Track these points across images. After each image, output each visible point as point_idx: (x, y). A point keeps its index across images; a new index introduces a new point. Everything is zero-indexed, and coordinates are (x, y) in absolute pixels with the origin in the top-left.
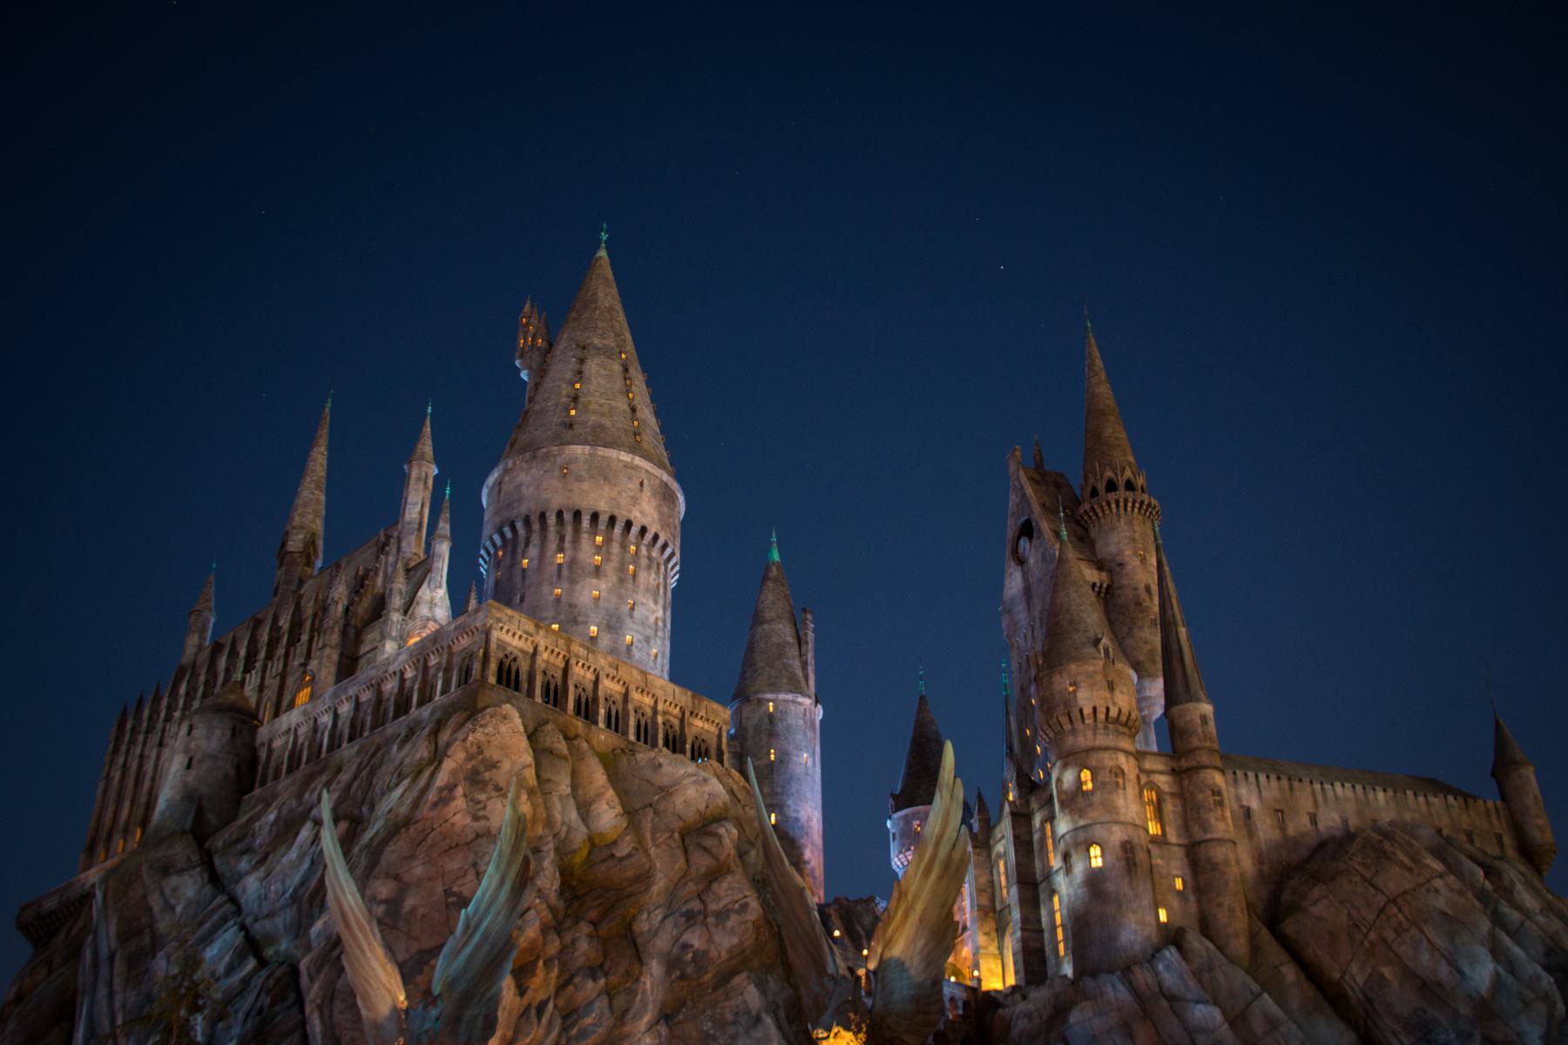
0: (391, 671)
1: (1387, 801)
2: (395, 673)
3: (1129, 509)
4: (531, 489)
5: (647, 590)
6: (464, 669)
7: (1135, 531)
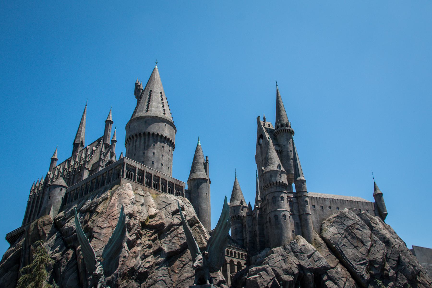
0: (100, 174)
1: (348, 203)
2: (101, 175)
3: (287, 132)
4: (137, 127)
5: (166, 152)
6: (118, 174)
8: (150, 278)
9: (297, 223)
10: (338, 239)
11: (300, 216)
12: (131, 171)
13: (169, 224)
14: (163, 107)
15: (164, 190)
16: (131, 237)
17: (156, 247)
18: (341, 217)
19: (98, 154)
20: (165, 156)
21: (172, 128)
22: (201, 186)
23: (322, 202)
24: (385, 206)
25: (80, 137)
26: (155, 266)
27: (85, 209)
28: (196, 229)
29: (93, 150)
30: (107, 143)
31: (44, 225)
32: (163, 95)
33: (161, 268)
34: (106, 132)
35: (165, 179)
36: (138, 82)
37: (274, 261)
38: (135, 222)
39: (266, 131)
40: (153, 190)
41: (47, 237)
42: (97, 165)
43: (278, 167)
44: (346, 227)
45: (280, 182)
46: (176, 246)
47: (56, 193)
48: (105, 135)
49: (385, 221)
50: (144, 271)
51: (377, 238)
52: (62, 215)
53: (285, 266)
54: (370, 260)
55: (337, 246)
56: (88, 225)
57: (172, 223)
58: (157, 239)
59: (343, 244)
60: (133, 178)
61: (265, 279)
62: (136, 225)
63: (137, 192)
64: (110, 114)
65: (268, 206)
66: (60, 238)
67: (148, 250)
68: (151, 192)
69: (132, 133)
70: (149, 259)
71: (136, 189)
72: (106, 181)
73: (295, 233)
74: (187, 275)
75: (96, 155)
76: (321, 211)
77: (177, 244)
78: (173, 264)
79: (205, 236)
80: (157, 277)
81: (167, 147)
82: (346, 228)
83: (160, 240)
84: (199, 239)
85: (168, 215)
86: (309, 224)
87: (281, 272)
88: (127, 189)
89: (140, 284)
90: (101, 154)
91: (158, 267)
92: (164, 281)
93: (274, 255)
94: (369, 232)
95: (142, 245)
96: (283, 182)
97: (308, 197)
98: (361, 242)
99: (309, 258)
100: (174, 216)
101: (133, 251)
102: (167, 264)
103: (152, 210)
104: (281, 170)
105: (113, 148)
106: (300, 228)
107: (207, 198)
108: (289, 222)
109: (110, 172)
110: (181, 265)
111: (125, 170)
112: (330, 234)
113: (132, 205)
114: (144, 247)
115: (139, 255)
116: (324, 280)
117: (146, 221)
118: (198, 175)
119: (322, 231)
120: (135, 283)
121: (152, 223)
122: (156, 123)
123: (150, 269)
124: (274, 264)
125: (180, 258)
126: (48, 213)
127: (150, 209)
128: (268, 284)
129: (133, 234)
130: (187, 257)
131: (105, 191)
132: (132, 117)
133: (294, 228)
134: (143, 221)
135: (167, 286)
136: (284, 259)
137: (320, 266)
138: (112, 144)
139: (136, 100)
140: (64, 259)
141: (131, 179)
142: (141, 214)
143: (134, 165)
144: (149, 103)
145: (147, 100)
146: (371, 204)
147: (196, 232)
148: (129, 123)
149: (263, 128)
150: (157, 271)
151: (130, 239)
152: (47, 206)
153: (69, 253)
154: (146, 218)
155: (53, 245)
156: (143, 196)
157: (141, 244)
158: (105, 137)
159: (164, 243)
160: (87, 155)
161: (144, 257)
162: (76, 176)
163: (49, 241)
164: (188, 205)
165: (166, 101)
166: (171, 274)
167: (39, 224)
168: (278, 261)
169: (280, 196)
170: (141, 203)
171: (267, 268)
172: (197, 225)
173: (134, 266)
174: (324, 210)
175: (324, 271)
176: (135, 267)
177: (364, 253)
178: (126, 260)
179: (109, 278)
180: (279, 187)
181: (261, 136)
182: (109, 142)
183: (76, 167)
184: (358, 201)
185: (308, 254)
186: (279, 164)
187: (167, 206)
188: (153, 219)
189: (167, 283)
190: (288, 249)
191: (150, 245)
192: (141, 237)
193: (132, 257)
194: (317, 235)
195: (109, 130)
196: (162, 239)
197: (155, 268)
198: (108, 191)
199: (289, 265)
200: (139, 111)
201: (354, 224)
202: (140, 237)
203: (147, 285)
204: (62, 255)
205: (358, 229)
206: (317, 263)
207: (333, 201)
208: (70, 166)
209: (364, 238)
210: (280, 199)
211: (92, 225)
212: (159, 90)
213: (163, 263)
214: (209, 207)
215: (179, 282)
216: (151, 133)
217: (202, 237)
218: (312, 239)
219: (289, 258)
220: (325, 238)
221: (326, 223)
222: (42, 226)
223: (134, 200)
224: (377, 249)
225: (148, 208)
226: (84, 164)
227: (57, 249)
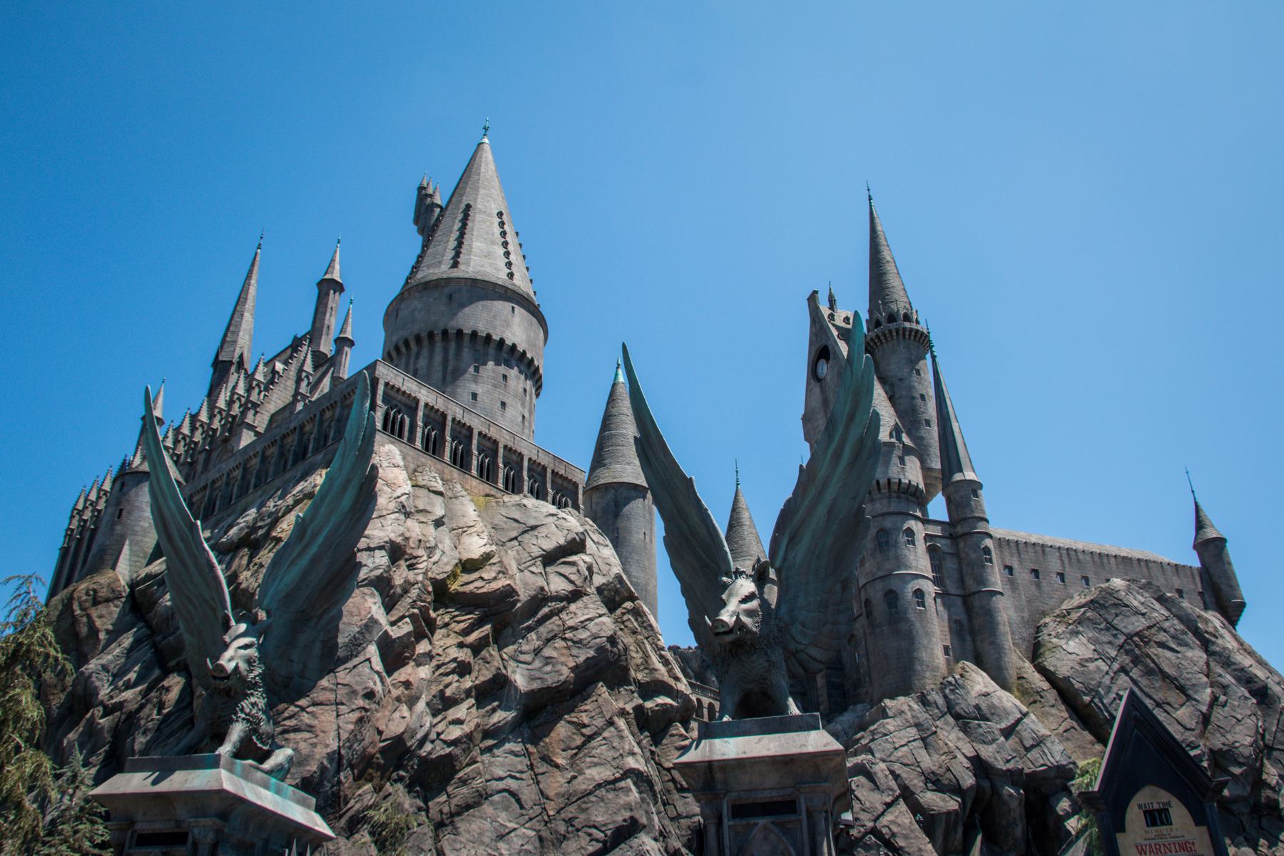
0: (292, 427)
1: (1117, 564)
2: (295, 428)
3: (907, 337)
4: (423, 313)
5: (516, 396)
7: (912, 354)
8: (464, 782)
9: (958, 622)
10: (1097, 676)
11: (966, 598)
12: (399, 412)
13: (533, 593)
14: (507, 254)
15: (513, 486)
16: (395, 628)
17: (484, 671)
18: (1103, 606)
19: (291, 384)
20: (512, 406)
21: (534, 320)
22: (626, 510)
23: (1034, 558)
24: (1235, 578)
25: (235, 342)
26: (481, 742)
27: (235, 539)
28: (625, 618)
29: (274, 372)
30: (322, 349)
31: (96, 602)
32: (506, 221)
33: (501, 749)
34: (318, 316)
35: (515, 451)
36: (428, 184)
37: (890, 743)
38: (409, 577)
39: (838, 337)
40: (475, 482)
41: (102, 643)
42: (287, 413)
43: (894, 433)
44: (1122, 639)
45: (903, 481)
46: (558, 671)
47: (141, 499)
48: (317, 325)
49: (1236, 627)
50: (442, 753)
51: (1228, 679)
52: (157, 568)
53: (928, 761)
54: (1211, 750)
55: (1096, 700)
56: (241, 584)
57: (542, 589)
58: (488, 645)
59: (1117, 694)
60: (406, 434)
61: (868, 804)
62: (416, 586)
63: (420, 479)
64: (333, 260)
66: (146, 643)
67: (457, 681)
68: (467, 487)
69: (404, 333)
70: (460, 711)
71: (415, 471)
72: (311, 446)
73: (951, 653)
74: (599, 773)
75: (283, 386)
76: (1034, 587)
77: (563, 664)
78: (547, 735)
79: (659, 643)
80: (487, 781)
81: (517, 380)
82: (1122, 641)
83: (500, 649)
84: (637, 652)
85: (528, 564)
86: (998, 624)
88: (385, 464)
89: (426, 802)
90: (299, 381)
91: (490, 742)
92: (513, 794)
93: (890, 724)
94: (1201, 657)
95: (434, 663)
96: (913, 483)
97: (990, 536)
98: (1177, 687)
99: (1007, 738)
100: (548, 569)
101: (403, 679)
102: (527, 733)
103: (471, 544)
104: (904, 444)
105: (340, 364)
106: (969, 638)
108: (935, 615)
109: (328, 415)
110: (574, 739)
111: (379, 402)
112: (1069, 660)
113: (402, 517)
114: (442, 670)
115: (423, 696)
116: (1061, 813)
117: (448, 577)
119: (1042, 650)
120: (407, 797)
121: (471, 587)
122: (482, 300)
123: (464, 750)
124: (892, 753)
125: (573, 715)
126: (111, 563)
127: (466, 539)
129: (403, 617)
130: (598, 710)
131: (304, 477)
132: (407, 283)
133: (948, 637)
134: (439, 577)
135: (524, 812)
136: (923, 739)
137: (1042, 765)
138: (339, 351)
139: (418, 240)
140: (149, 706)
141: (401, 435)
142: (431, 552)
143: (411, 388)
144: (460, 252)
145: (456, 234)
146: (1189, 573)
147: (626, 630)
148: (394, 303)
149: (830, 326)
150: (486, 757)
151: (391, 633)
152: (108, 543)
153: (169, 687)
154: (449, 568)
155: (118, 667)
156: (440, 494)
157: (429, 656)
158: (315, 334)
159: (512, 658)
160: (255, 383)
161: (443, 703)
162: (214, 454)
163: (108, 654)
164: (596, 540)
165: (517, 241)
166: (541, 770)
167: (79, 598)
168: (903, 743)
169: (902, 528)
170: (434, 518)
171: (873, 763)
172: (628, 605)
173: (403, 733)
174: (1044, 584)
175: (1058, 781)
176: (406, 736)
177: (1192, 723)
178: (374, 706)
179: (310, 771)
180: (899, 497)
181: (821, 352)
182: (327, 347)
183: (216, 424)
184: (1150, 561)
185: (1003, 725)
186: (897, 423)
187: (526, 532)
188: (475, 575)
189: (524, 803)
190: (935, 703)
191: (463, 662)
192: (433, 636)
193: (398, 699)
194: (1024, 662)
195: (329, 310)
196: (507, 646)
197: (481, 745)
198: (319, 472)
199: (943, 757)
200: (429, 267)
201: (1150, 627)
202: (427, 631)
203: (452, 806)
204: (145, 694)
205: (1162, 645)
206: (1034, 754)
207: (1068, 555)
208: (198, 424)
209: (1187, 676)
210: (903, 539)
211: (252, 580)
212: (493, 206)
213: (512, 732)
215: (568, 799)
216: (467, 331)
217: (649, 647)
218: (1012, 674)
219: (942, 734)
220: (1053, 673)
221: (1052, 625)
222: (87, 605)
223: (408, 498)
224: (1234, 714)
225: (459, 536)
226: (244, 414)
227: (132, 676)
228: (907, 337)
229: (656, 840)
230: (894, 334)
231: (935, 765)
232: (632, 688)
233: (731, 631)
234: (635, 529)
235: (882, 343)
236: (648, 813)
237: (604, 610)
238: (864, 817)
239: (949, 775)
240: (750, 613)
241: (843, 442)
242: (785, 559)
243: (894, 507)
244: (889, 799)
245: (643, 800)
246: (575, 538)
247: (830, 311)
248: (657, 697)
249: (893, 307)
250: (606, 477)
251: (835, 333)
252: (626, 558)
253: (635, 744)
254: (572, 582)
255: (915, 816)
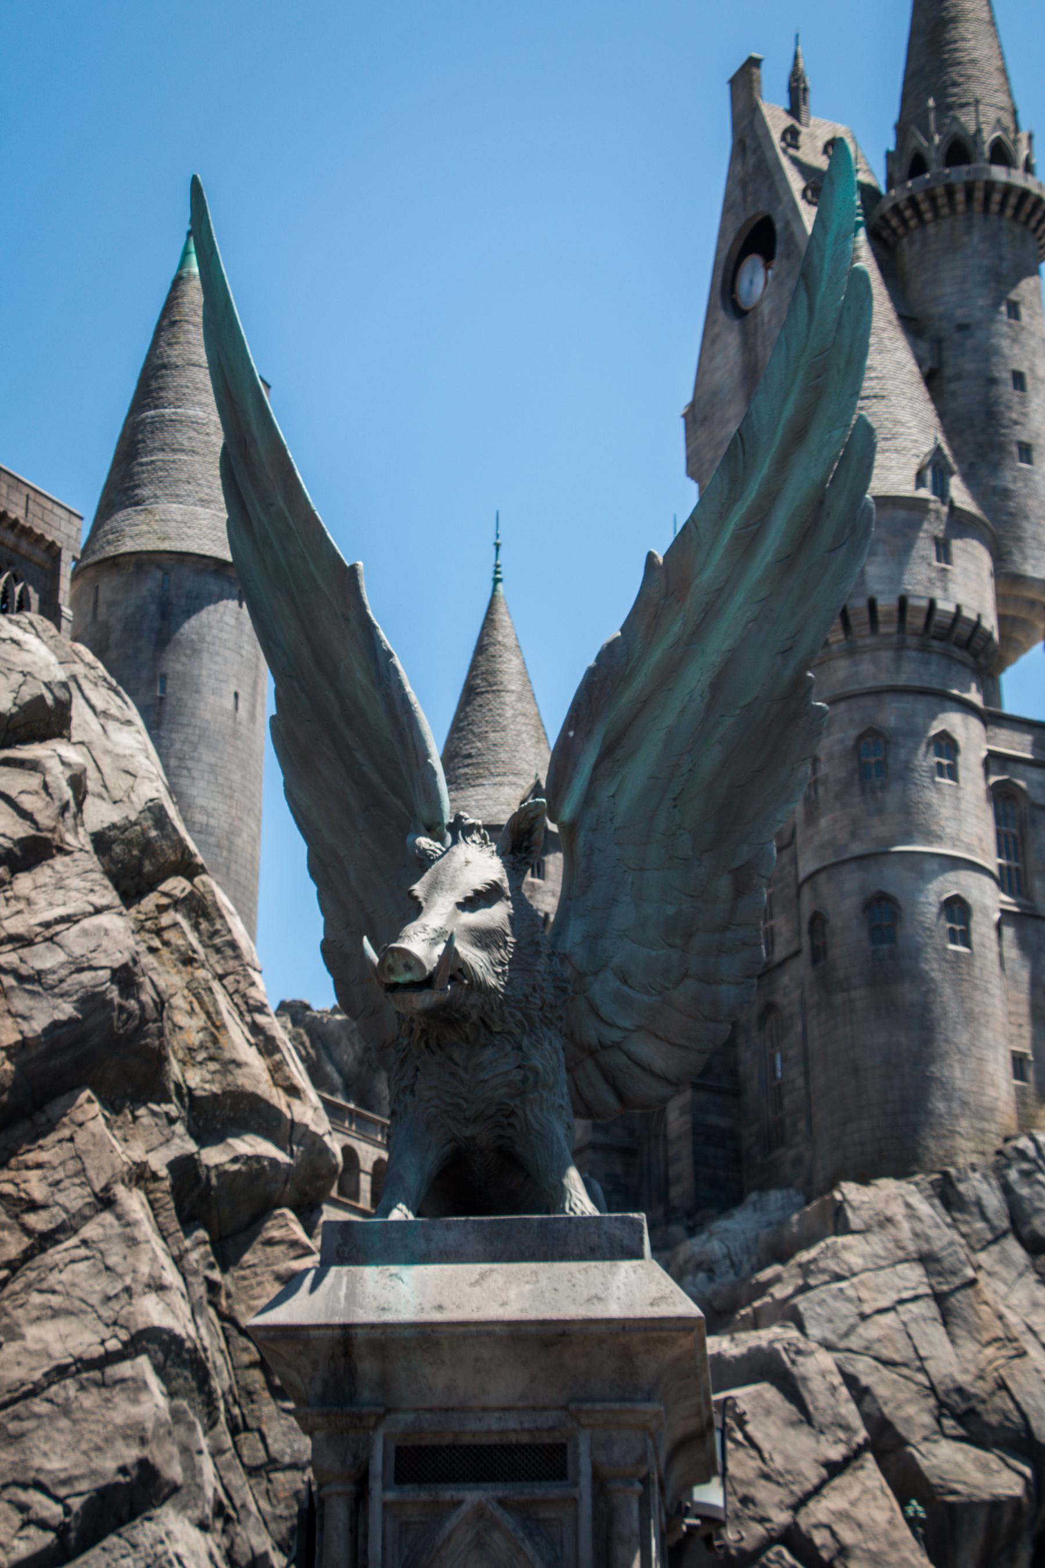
7: (1001, 258)
22: (190, 627)
28: (165, 920)
37: (849, 1300)
39: (804, 196)
43: (929, 475)
45: (941, 605)
65: (811, 815)
73: (1031, 1075)
74: (63, 1338)
79: (252, 992)
84: (192, 1013)
87: (911, 1410)
104: (953, 508)
107: (235, 734)
108: (997, 969)
118: (171, 529)
124: (852, 1328)
128: (799, 1504)
130: (72, 1166)
133: (1027, 1031)
136: (939, 1298)
147: (165, 952)
164: (100, 705)
169: (926, 728)
171: (799, 1352)
172: (177, 885)
180: (924, 648)
190: (979, 1204)
199: (990, 1351)
210: (926, 760)
214: (249, 811)
217: (223, 1002)
219: (990, 1288)
228: (994, 207)
229: (203, 1526)
230: (960, 197)
231: (966, 1371)
232: (173, 1109)
233: (427, 983)
234: (212, 682)
235: (922, 223)
236: (188, 1452)
237: (109, 896)
238: (766, 1494)
239: (1002, 1401)
240: (484, 938)
241: (770, 496)
242: (588, 800)
243: (908, 674)
244: (836, 1453)
245: (177, 1415)
246: (41, 698)
247: (789, 121)
248: (237, 1135)
249: (967, 119)
250: (139, 535)
251: (796, 183)
252: (181, 759)
253: (166, 1261)
254: (26, 815)
255: (903, 1503)
